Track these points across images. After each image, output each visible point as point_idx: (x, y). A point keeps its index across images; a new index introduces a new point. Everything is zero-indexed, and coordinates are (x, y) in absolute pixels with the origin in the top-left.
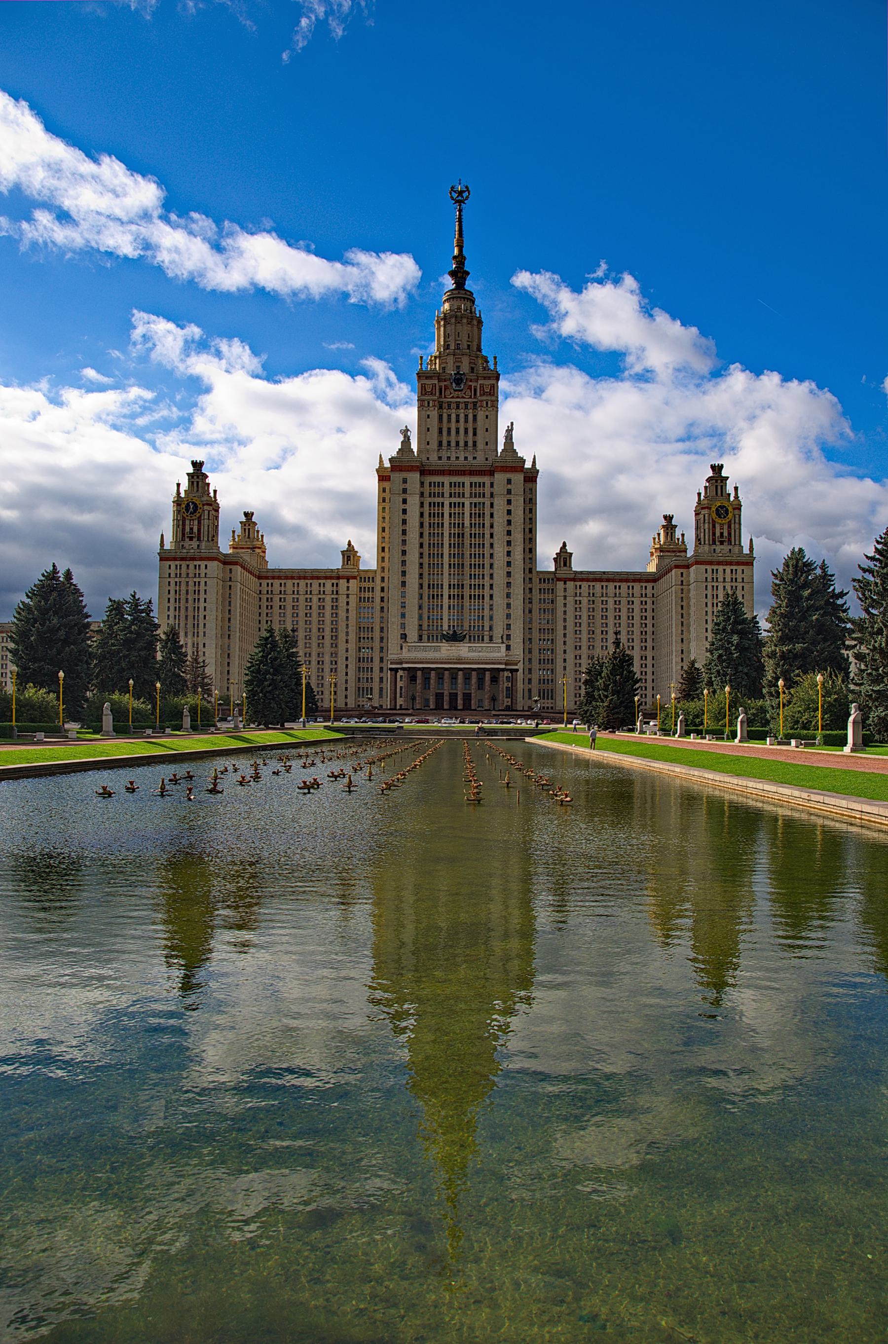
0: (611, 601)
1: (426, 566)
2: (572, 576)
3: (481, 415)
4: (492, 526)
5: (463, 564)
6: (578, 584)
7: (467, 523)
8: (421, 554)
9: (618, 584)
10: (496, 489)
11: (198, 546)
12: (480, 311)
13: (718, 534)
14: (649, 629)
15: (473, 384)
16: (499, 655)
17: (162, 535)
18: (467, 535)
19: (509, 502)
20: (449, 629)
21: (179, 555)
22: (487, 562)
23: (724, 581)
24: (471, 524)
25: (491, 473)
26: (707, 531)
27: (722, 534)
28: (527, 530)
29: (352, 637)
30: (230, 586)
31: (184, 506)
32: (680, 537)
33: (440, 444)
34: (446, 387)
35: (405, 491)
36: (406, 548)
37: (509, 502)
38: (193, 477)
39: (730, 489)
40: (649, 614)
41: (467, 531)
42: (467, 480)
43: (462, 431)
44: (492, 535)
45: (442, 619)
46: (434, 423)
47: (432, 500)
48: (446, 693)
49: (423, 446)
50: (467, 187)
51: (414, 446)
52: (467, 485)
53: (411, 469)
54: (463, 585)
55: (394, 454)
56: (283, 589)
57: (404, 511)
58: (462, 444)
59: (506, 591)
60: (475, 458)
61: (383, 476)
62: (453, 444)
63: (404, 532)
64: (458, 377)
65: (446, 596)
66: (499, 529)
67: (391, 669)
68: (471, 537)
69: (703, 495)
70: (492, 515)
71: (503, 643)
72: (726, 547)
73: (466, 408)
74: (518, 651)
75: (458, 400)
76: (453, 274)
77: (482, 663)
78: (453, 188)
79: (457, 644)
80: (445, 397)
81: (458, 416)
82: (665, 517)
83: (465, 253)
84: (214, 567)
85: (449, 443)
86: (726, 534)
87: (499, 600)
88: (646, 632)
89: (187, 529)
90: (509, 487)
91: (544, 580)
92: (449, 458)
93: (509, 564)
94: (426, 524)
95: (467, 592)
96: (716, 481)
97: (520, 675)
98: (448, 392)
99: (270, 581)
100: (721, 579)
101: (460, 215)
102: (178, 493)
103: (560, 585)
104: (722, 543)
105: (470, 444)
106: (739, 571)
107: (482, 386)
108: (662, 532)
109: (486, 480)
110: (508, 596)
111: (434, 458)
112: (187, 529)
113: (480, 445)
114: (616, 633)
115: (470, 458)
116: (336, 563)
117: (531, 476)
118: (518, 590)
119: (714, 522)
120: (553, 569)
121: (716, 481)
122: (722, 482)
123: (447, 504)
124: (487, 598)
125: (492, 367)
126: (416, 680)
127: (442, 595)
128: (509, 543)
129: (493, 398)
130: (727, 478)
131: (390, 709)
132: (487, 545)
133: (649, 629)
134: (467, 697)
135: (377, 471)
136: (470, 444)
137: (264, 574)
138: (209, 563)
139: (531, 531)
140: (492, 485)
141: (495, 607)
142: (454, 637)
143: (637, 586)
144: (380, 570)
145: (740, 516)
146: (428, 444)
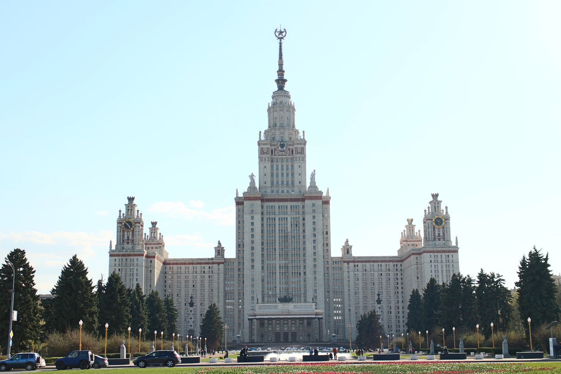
0: (376, 274)
1: (265, 256)
2: (352, 259)
3: (296, 165)
4: (304, 231)
5: (287, 254)
6: (356, 264)
7: (289, 230)
8: (263, 248)
9: (380, 264)
10: (306, 209)
11: (132, 247)
12: (294, 103)
13: (437, 234)
14: (400, 290)
15: (291, 147)
16: (311, 309)
17: (111, 241)
18: (290, 237)
19: (314, 217)
20: (280, 294)
21: (121, 253)
22: (302, 253)
23: (442, 262)
24: (292, 230)
25: (303, 200)
26: (430, 233)
27: (439, 234)
28: (325, 233)
29: (222, 299)
30: (151, 271)
31: (123, 224)
32: (418, 232)
34: (275, 150)
35: (252, 211)
36: (254, 245)
37: (314, 217)
38: (128, 207)
39: (443, 207)
40: (399, 281)
41: (290, 234)
42: (289, 204)
43: (285, 175)
44: (304, 237)
45: (275, 287)
46: (268, 171)
47: (269, 216)
48: (282, 332)
49: (262, 185)
50: (285, 30)
51: (257, 185)
52: (289, 207)
53: (256, 199)
54: (288, 266)
55: (246, 191)
56: (179, 270)
57: (252, 224)
58: (285, 183)
59: (313, 270)
60: (293, 191)
61: (239, 202)
62: (280, 183)
63: (252, 236)
64: (282, 143)
65: (278, 274)
67: (249, 319)
68: (292, 238)
69: (427, 211)
70: (304, 224)
71: (313, 303)
72: (442, 242)
73: (287, 161)
75: (283, 157)
76: (277, 81)
77: (302, 315)
78: (276, 30)
79: (287, 304)
80: (275, 155)
81: (282, 166)
82: (408, 220)
83: (284, 69)
85: (277, 182)
86: (441, 234)
87: (310, 276)
88: (398, 292)
89: (126, 238)
90: (314, 208)
91: (336, 262)
92: (278, 191)
93: (315, 253)
94: (265, 231)
95: (290, 270)
96: (435, 204)
97: (324, 320)
98: (276, 152)
99: (171, 266)
100: (439, 261)
102: (120, 216)
104: (439, 240)
105: (290, 182)
106: (450, 256)
107: (296, 148)
108: (405, 229)
109: (300, 204)
110: (315, 272)
111: (269, 191)
112: (126, 238)
113: (296, 183)
114: (379, 295)
115: (290, 191)
116: (212, 254)
117: (326, 202)
118: (320, 269)
120: (341, 256)
121: (435, 204)
122: (438, 204)
124: (302, 274)
125: (302, 138)
126: (264, 325)
127: (275, 273)
128: (314, 241)
129: (303, 155)
130: (442, 201)
131: (249, 343)
132: (301, 243)
133: (400, 290)
134: (294, 334)
135: (235, 199)
136: (290, 182)
137: (168, 262)
138: (139, 258)
139: (327, 233)
140: (303, 207)
141: (307, 280)
142: (285, 300)
144: (237, 258)
145: (449, 223)
146: (265, 183)
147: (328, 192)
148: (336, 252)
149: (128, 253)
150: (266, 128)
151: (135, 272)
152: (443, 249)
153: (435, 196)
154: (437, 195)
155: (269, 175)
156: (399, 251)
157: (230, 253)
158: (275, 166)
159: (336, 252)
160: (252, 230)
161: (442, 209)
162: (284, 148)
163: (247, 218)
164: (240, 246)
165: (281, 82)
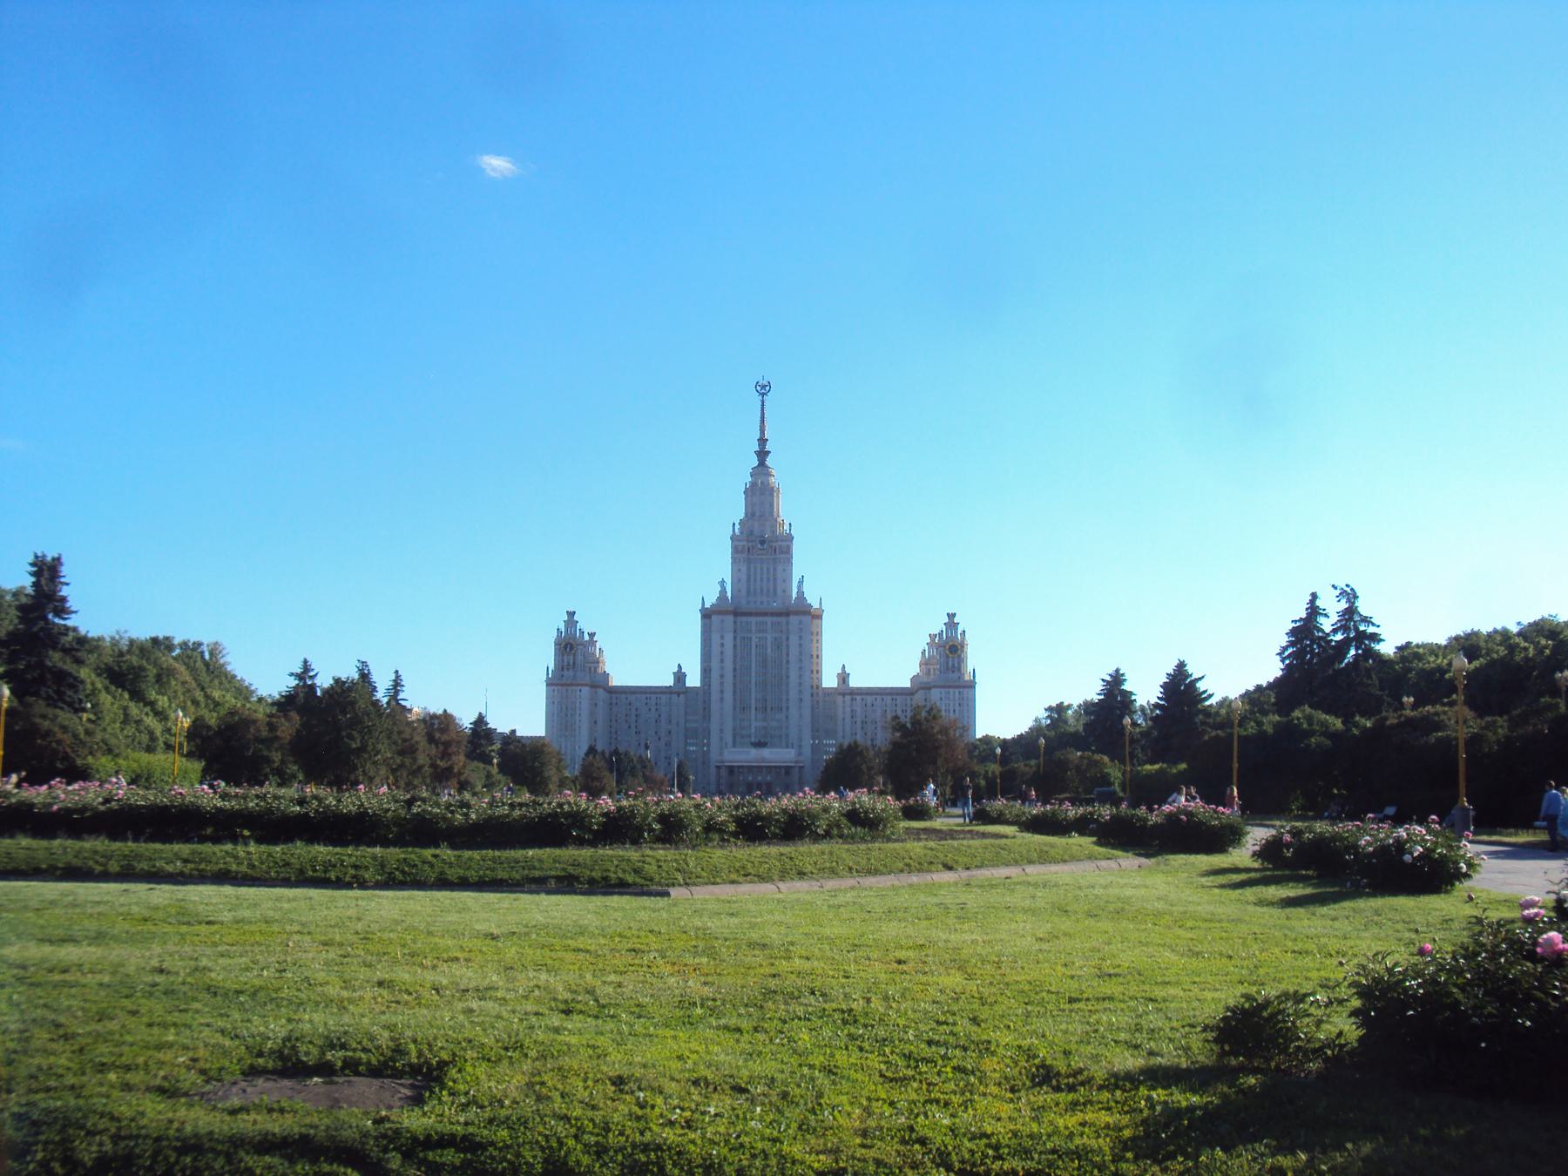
3: (780, 568)
4: (788, 655)
7: (769, 651)
13: (950, 663)
19: (801, 637)
21: (560, 682)
25: (787, 614)
27: (953, 665)
33: (748, 591)
37: (801, 637)
41: (769, 659)
42: (769, 619)
43: (765, 580)
44: (788, 662)
51: (729, 595)
53: (726, 613)
57: (722, 645)
61: (707, 614)
65: (753, 711)
66: (793, 657)
70: (788, 646)
72: (956, 675)
74: (807, 751)
81: (762, 569)
84: (586, 690)
87: (793, 712)
89: (566, 664)
92: (755, 602)
93: (800, 684)
100: (951, 697)
101: (763, 405)
103: (840, 698)
104: (953, 672)
107: (780, 546)
109: (783, 620)
113: (779, 592)
116: (669, 681)
117: (818, 616)
119: (947, 657)
120: (835, 685)
123: (754, 638)
124: (784, 709)
140: (787, 623)
142: (760, 745)
143: (898, 697)
147: (821, 603)
148: (829, 681)
149: (569, 682)
150: (742, 515)
151: (578, 705)
152: (957, 684)
153: (951, 616)
154: (954, 615)
155: (744, 577)
156: (913, 679)
157: (694, 680)
158: (752, 570)
159: (829, 681)
160: (722, 653)
161: (959, 632)
162: (765, 546)
163: (716, 638)
164: (706, 672)
165: (762, 454)
